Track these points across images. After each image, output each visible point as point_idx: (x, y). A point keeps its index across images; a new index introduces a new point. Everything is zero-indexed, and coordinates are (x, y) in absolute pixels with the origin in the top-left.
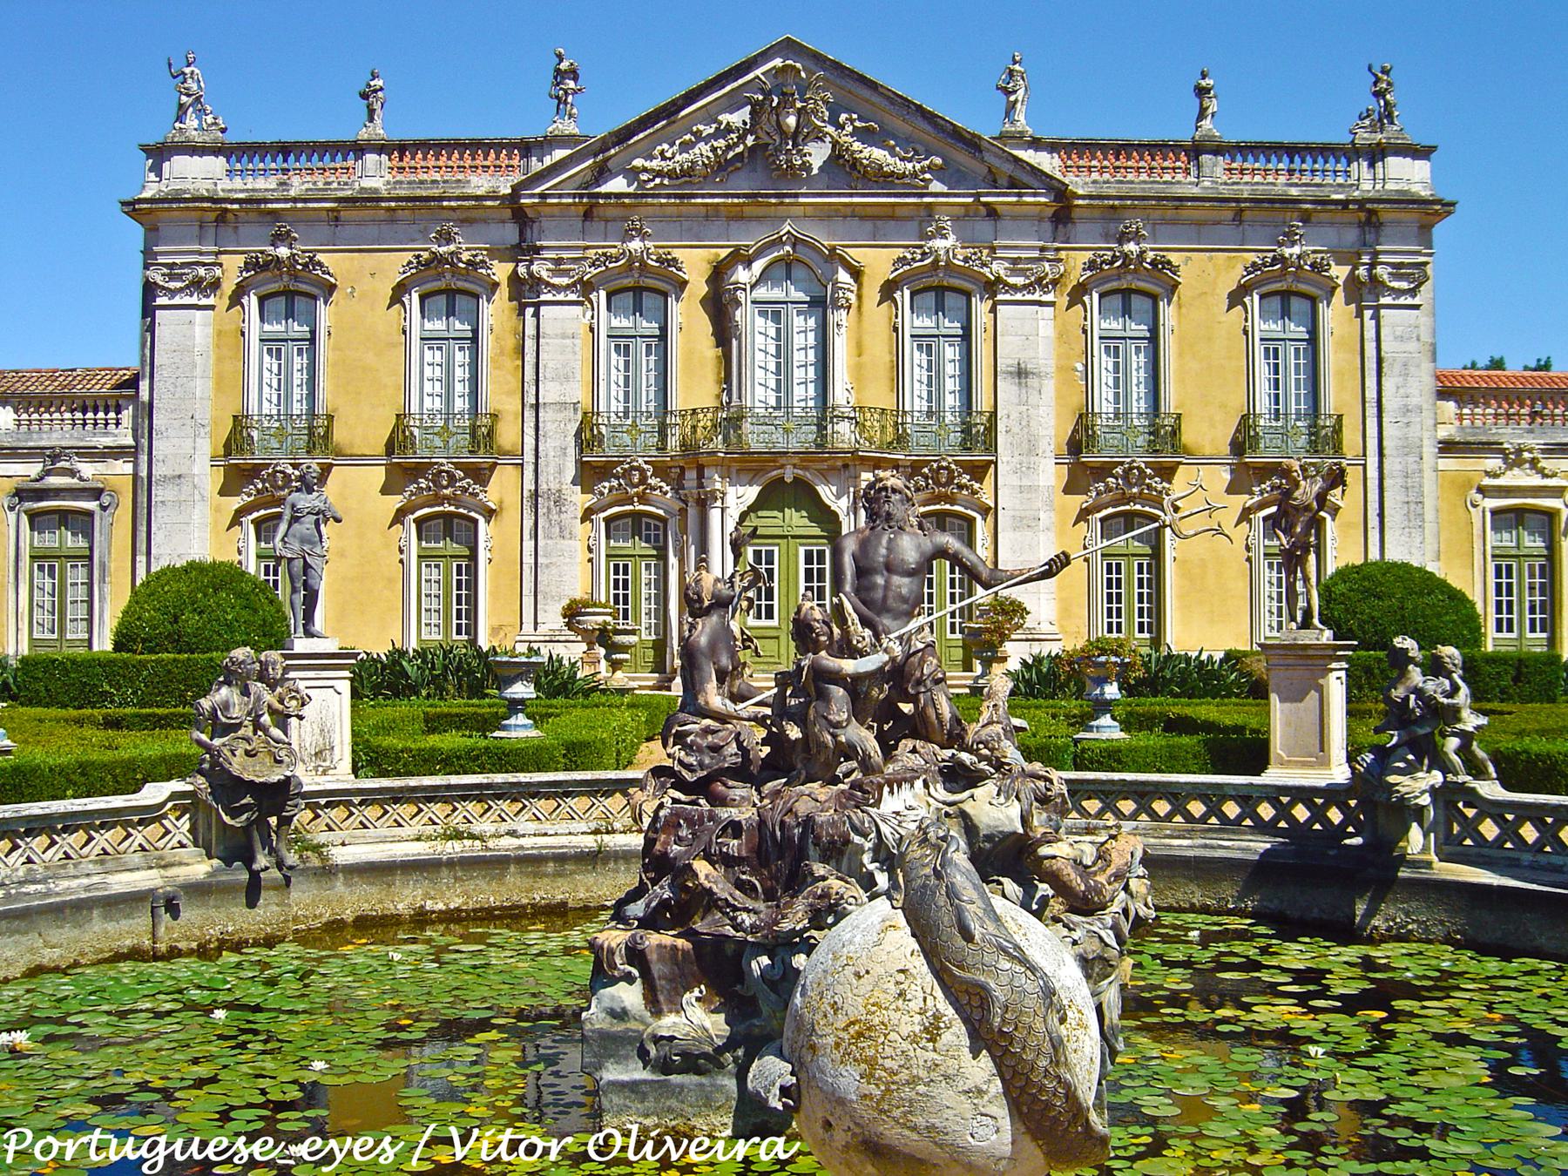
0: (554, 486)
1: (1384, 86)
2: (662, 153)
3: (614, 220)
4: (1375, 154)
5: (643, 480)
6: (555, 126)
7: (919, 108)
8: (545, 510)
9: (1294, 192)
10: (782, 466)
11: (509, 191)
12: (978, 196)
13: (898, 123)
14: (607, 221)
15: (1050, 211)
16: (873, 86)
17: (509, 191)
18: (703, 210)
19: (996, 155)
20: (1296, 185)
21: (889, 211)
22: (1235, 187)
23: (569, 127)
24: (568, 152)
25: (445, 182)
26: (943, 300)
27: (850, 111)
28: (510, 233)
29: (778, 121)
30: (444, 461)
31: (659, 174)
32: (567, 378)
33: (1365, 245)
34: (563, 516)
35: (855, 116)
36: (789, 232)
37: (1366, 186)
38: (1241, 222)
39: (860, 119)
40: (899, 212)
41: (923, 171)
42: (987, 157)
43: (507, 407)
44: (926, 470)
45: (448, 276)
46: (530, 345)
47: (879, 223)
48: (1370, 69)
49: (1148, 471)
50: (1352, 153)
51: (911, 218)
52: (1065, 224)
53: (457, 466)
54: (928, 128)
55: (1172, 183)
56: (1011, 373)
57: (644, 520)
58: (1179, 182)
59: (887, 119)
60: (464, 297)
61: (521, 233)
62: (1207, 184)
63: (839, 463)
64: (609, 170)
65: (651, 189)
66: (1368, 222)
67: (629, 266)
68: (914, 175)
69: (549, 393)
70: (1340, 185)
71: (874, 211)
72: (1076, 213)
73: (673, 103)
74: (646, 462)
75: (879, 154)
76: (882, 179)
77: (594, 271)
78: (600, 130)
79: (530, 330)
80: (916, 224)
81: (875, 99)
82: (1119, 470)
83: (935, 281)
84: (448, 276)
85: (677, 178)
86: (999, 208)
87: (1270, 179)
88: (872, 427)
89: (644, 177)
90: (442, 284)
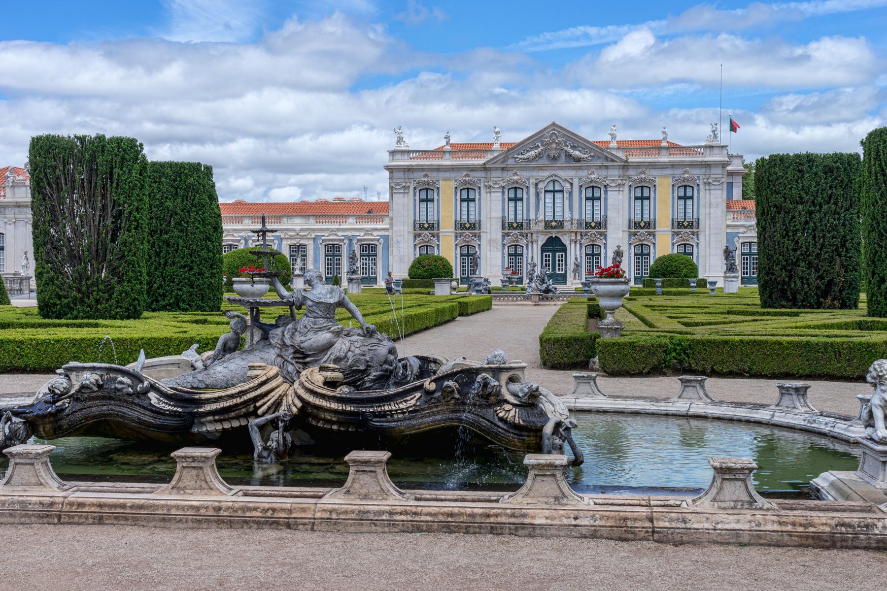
76: (578, 160)
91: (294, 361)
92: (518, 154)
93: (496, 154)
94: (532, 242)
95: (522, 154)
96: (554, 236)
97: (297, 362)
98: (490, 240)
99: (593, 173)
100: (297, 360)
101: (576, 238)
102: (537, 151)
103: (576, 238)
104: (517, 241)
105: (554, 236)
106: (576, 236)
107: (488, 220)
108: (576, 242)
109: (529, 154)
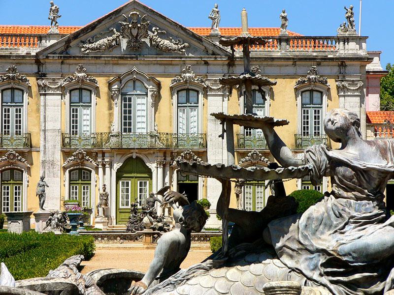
0: (51, 159)
1: (350, 14)
2: (89, 41)
3: (72, 64)
4: (346, 40)
5: (83, 158)
6: (50, 30)
7: (181, 26)
8: (48, 167)
9: (315, 54)
10: (132, 153)
11: (35, 54)
12: (201, 58)
13: (172, 31)
14: (70, 65)
15: (227, 62)
16: (164, 18)
17: (35, 54)
18: (104, 61)
19: (208, 44)
20: (316, 52)
21: (170, 62)
22: (294, 53)
23: (55, 30)
24: (55, 41)
25: (10, 49)
26: (189, 95)
27: (156, 26)
28: (35, 68)
29: (131, 31)
30: (12, 150)
31: (89, 49)
32: (56, 121)
33: (340, 73)
34: (54, 170)
35: (158, 28)
36: (134, 70)
37: (342, 52)
38: (295, 65)
39: (160, 29)
40: (173, 62)
41: (182, 48)
42: (204, 43)
43: (34, 130)
44: (182, 154)
45: (12, 84)
46: (42, 108)
47: (166, 66)
48: (345, 8)
49: (260, 154)
50: (338, 39)
51: (178, 65)
52: (232, 66)
53: (17, 152)
54: (183, 33)
55: (271, 51)
56: (212, 120)
57: (83, 171)
58: (273, 51)
59: (169, 29)
60: (17, 91)
61: (39, 68)
62: (283, 52)
63: (152, 152)
64: (70, 47)
65: (86, 54)
66: (342, 65)
67: (78, 82)
68: (179, 50)
69: (49, 126)
70: (332, 51)
71: (165, 62)
72: (236, 63)
73: (94, 23)
74: (84, 151)
75: (167, 42)
76: (168, 50)
77: (65, 83)
78: (69, 32)
79: (42, 103)
80: (179, 66)
81: (165, 22)
82: (250, 154)
83: (186, 87)
84: (12, 84)
85: (95, 50)
86: (209, 62)
87: (307, 49)
88: (163, 140)
89: (83, 50)
90: (10, 86)
91: (325, 280)
92: (84, 42)
93: (53, 42)
94: (104, 166)
95: (90, 43)
96: (134, 157)
97: (332, 282)
98: (44, 162)
99: (188, 71)
100: (331, 278)
101: (165, 159)
102: (110, 38)
103: (165, 159)
104: (83, 164)
105: (134, 157)
106: (165, 156)
107: (42, 133)
108: (164, 166)
109: (101, 42)
